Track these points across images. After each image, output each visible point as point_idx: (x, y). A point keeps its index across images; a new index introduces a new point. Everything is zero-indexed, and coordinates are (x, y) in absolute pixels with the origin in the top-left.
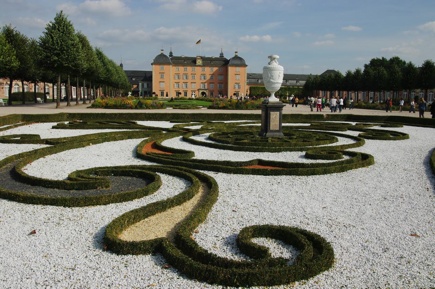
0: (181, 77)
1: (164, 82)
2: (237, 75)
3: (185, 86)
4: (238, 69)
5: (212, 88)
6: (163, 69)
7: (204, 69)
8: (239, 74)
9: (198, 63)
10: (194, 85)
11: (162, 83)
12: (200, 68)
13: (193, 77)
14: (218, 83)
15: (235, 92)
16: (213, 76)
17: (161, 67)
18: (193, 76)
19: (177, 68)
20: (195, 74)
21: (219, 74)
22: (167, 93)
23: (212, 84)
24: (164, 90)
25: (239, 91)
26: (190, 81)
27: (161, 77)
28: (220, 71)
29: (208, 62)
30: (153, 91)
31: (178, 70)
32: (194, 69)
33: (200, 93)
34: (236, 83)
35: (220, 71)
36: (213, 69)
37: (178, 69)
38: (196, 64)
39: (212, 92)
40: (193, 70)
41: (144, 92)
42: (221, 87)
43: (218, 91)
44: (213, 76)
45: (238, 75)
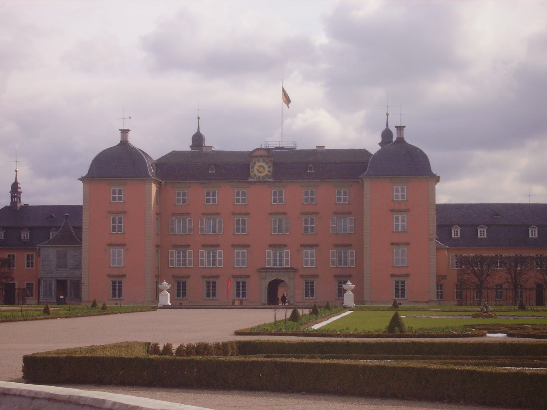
3: (209, 260)
5: (312, 264)
6: (120, 199)
7: (281, 194)
8: (407, 211)
9: (258, 174)
10: (243, 256)
11: (117, 250)
13: (238, 223)
14: (335, 246)
16: (312, 220)
17: (114, 193)
18: (238, 221)
19: (179, 194)
20: (247, 214)
21: (335, 213)
23: (309, 251)
27: (114, 228)
31: (184, 201)
32: (241, 197)
33: (265, 284)
35: (339, 200)
36: (312, 194)
37: (184, 195)
38: (248, 176)
39: (310, 280)
40: (238, 201)
43: (335, 276)
44: (312, 220)
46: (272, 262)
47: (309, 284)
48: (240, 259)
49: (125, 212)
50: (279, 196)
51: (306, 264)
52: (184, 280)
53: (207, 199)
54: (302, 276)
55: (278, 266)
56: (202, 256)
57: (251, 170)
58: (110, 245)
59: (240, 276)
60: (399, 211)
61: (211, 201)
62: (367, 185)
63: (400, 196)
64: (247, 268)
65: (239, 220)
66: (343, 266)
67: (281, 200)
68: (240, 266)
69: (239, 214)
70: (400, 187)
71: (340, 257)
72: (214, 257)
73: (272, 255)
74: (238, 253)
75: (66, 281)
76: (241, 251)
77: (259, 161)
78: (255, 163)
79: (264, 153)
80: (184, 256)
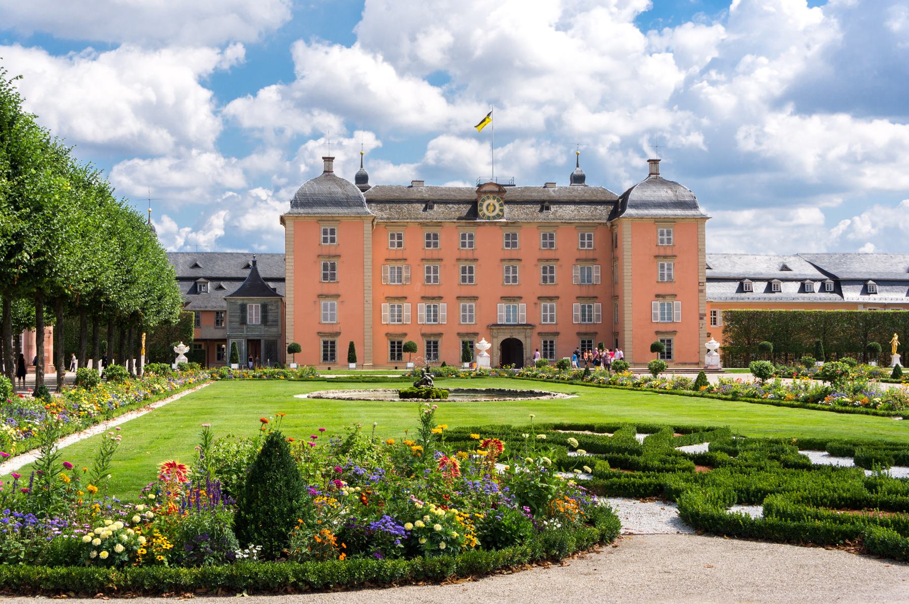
5: (552, 320)
6: (333, 240)
9: (487, 214)
10: (471, 311)
11: (329, 302)
15: (658, 339)
17: (325, 232)
20: (476, 260)
23: (548, 305)
28: (583, 244)
30: (290, 340)
31: (400, 245)
32: (467, 241)
34: (658, 296)
37: (400, 237)
42: (590, 316)
43: (578, 334)
44: (552, 268)
46: (505, 318)
47: (548, 343)
48: (468, 314)
50: (512, 239)
51: (545, 320)
52: (399, 339)
53: (427, 243)
55: (511, 323)
57: (479, 208)
58: (321, 296)
59: (467, 334)
60: (665, 257)
61: (432, 244)
63: (666, 240)
64: (476, 324)
65: (465, 267)
66: (587, 322)
67: (515, 245)
68: (468, 323)
69: (466, 260)
70: (665, 230)
71: (583, 311)
72: (435, 311)
73: (505, 309)
74: (464, 307)
75: (259, 341)
76: (468, 305)
77: (488, 198)
78: (484, 201)
79: (497, 189)
80: (400, 311)
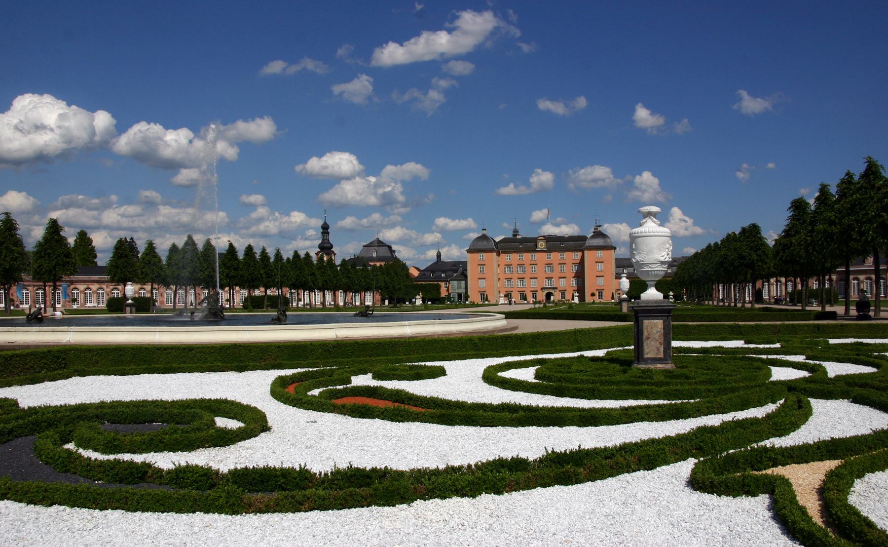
0: (515, 269)
1: (484, 279)
2: (598, 264)
4: (599, 254)
8: (603, 262)
11: (482, 280)
12: (545, 255)
20: (536, 264)
22: (487, 295)
24: (485, 292)
25: (603, 290)
26: (527, 275)
29: (556, 244)
33: (544, 294)
41: (458, 294)
45: (600, 264)
49: (484, 265)
54: (560, 291)
56: (518, 282)
62: (586, 252)
79: (543, 238)
